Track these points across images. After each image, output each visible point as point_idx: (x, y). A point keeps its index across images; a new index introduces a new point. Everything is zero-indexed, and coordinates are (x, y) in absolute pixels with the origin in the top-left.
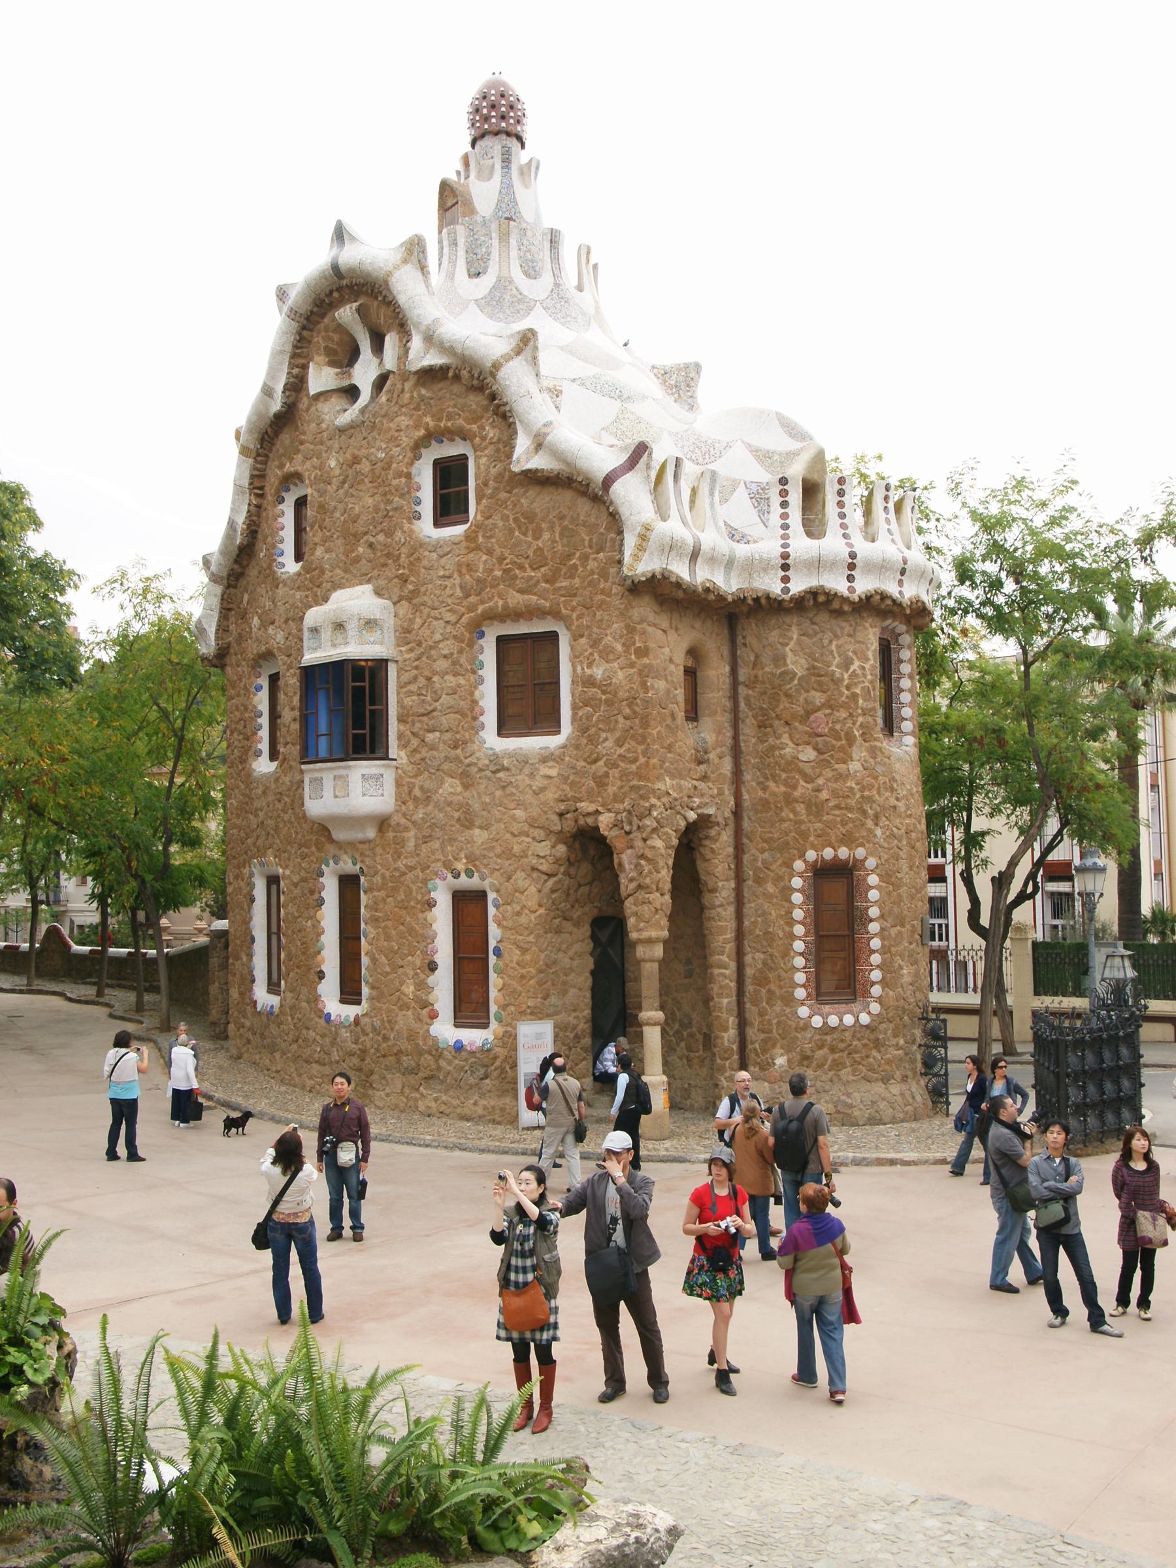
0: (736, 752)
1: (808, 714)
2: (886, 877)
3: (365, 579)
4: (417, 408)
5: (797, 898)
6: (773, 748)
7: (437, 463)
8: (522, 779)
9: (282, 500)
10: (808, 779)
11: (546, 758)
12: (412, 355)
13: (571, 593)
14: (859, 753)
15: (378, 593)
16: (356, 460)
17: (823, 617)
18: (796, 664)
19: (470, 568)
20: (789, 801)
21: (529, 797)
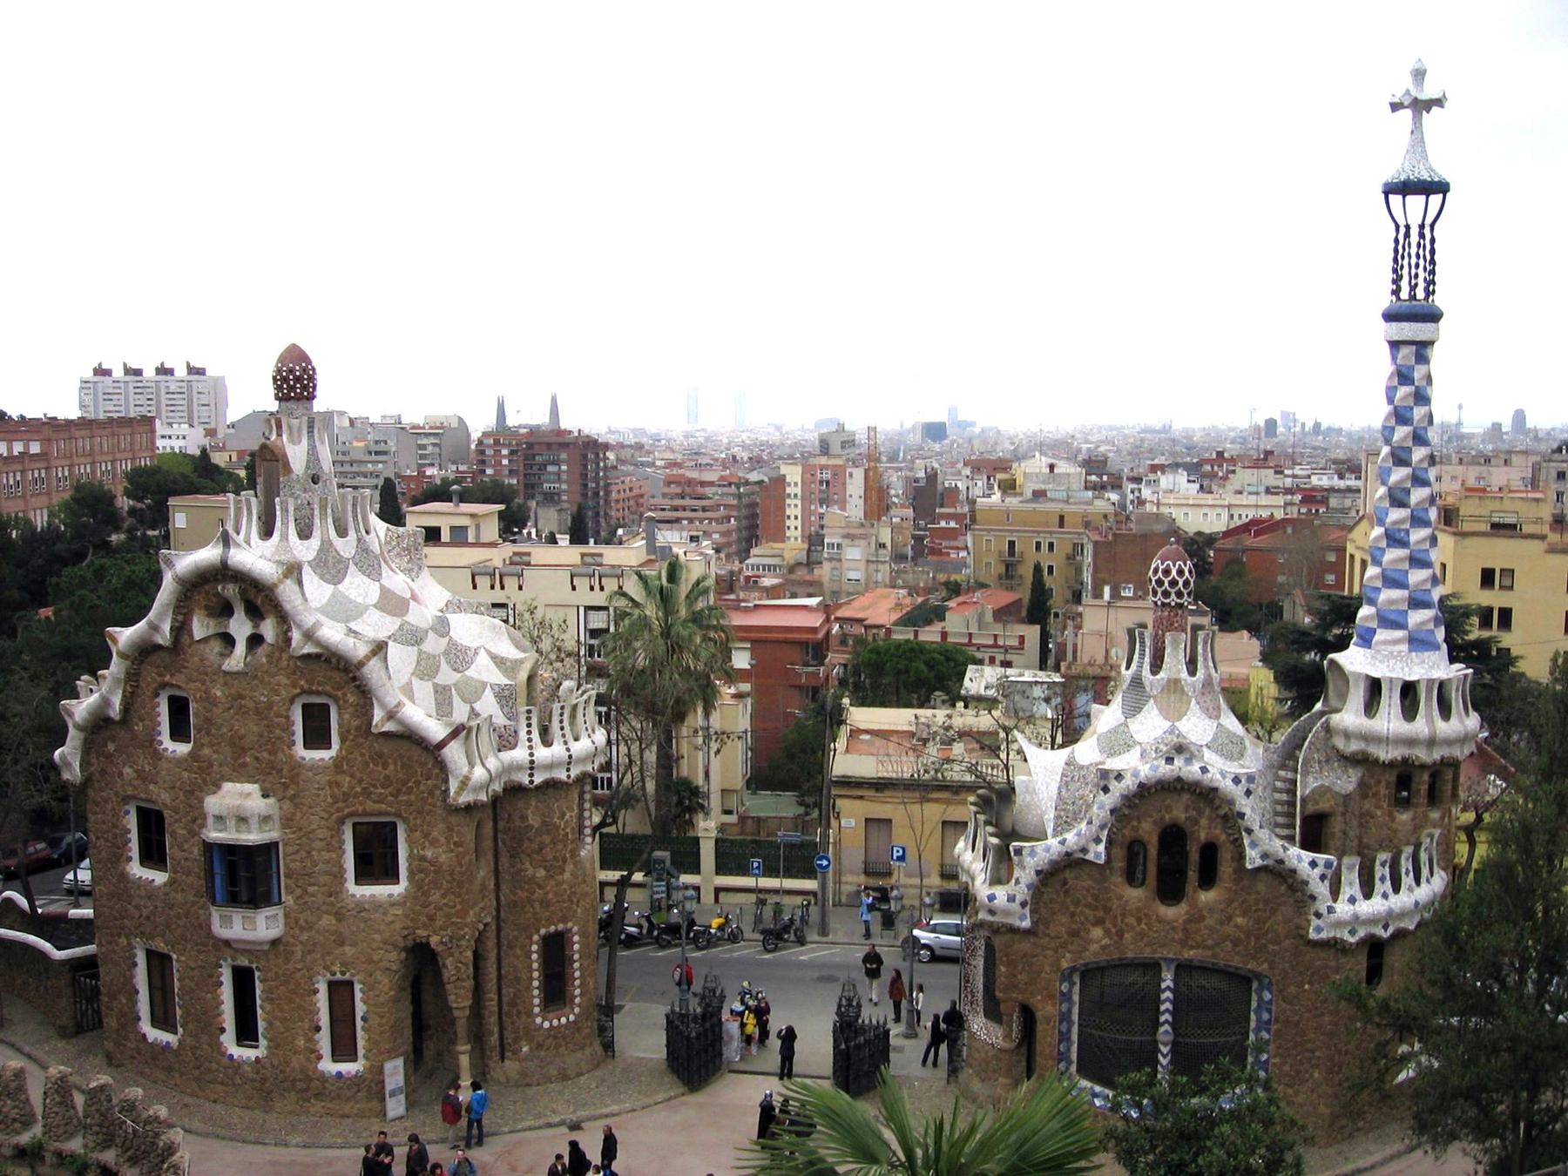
0: (497, 872)
1: (541, 849)
2: (583, 934)
3: (250, 779)
4: (294, 673)
5: (535, 956)
6: (520, 871)
9: (157, 695)
10: (541, 887)
11: (393, 903)
12: (294, 644)
14: (569, 867)
16: (241, 697)
17: (550, 791)
18: (534, 820)
19: (338, 784)
20: (530, 901)
21: (383, 927)
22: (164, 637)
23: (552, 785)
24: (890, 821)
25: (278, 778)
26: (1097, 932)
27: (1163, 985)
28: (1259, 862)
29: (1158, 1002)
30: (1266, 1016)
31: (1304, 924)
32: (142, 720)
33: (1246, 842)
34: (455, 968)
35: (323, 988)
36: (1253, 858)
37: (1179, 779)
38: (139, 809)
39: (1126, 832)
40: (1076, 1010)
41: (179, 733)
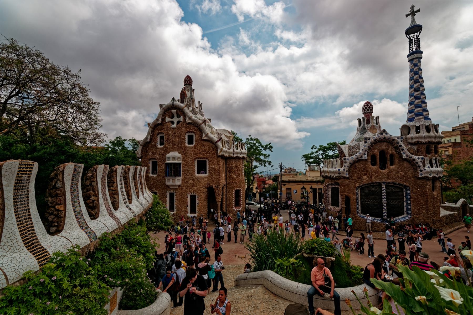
0: (226, 176)
3: (176, 151)
7: (188, 135)
8: (202, 180)
13: (209, 156)
14: (240, 176)
15: (179, 153)
16: (175, 133)
17: (237, 159)
18: (234, 165)
19: (194, 151)
20: (233, 182)
22: (160, 121)
23: (238, 158)
24: (290, 189)
25: (183, 150)
26: (365, 177)
27: (383, 189)
28: (406, 157)
29: (382, 193)
30: (409, 197)
31: (417, 174)
32: (154, 141)
33: (402, 152)
34: (218, 192)
35: (189, 197)
36: (404, 156)
37: (385, 138)
38: (152, 162)
39: (371, 153)
40: (359, 197)
41: (161, 144)
